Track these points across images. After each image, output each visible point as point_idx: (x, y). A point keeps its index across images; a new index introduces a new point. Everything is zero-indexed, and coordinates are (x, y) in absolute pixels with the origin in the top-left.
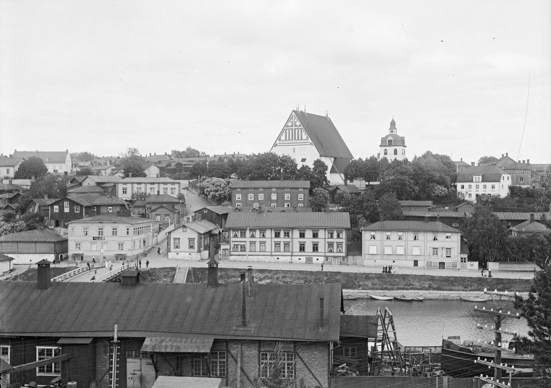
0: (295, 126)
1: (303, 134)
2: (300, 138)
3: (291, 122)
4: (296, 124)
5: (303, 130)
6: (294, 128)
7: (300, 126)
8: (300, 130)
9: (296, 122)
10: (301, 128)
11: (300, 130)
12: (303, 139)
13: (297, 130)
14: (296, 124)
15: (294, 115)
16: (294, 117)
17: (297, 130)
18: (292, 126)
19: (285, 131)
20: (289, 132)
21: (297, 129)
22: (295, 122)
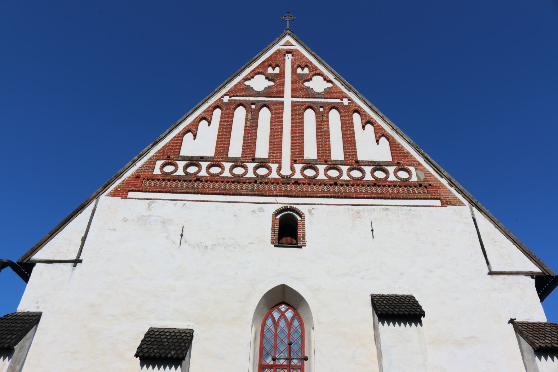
5: (356, 117)
11: (334, 117)
16: (289, 59)
19: (217, 113)
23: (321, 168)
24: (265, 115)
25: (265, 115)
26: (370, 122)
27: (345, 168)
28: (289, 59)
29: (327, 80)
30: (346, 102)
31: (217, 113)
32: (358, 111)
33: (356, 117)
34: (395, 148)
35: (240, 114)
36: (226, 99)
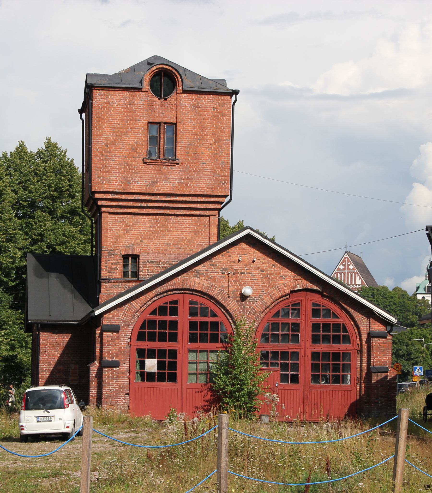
0: (349, 269)
1: (358, 278)
2: (353, 283)
3: (343, 265)
4: (350, 267)
5: (357, 274)
6: (346, 271)
7: (353, 269)
8: (353, 274)
9: (349, 265)
10: (354, 272)
11: (353, 274)
12: (357, 283)
13: (350, 274)
14: (350, 267)
15: (347, 258)
16: (346, 259)
17: (350, 274)
18: (344, 269)
19: (335, 274)
20: (341, 275)
21: (350, 272)
22: (348, 265)
23: (351, 285)
24: (343, 274)
25: (343, 274)
26: (359, 276)
27: (354, 285)
28: (346, 259)
29: (353, 266)
30: (356, 271)
31: (335, 274)
32: (358, 273)
33: (357, 274)
34: (362, 281)
35: (339, 274)
36: (336, 271)
